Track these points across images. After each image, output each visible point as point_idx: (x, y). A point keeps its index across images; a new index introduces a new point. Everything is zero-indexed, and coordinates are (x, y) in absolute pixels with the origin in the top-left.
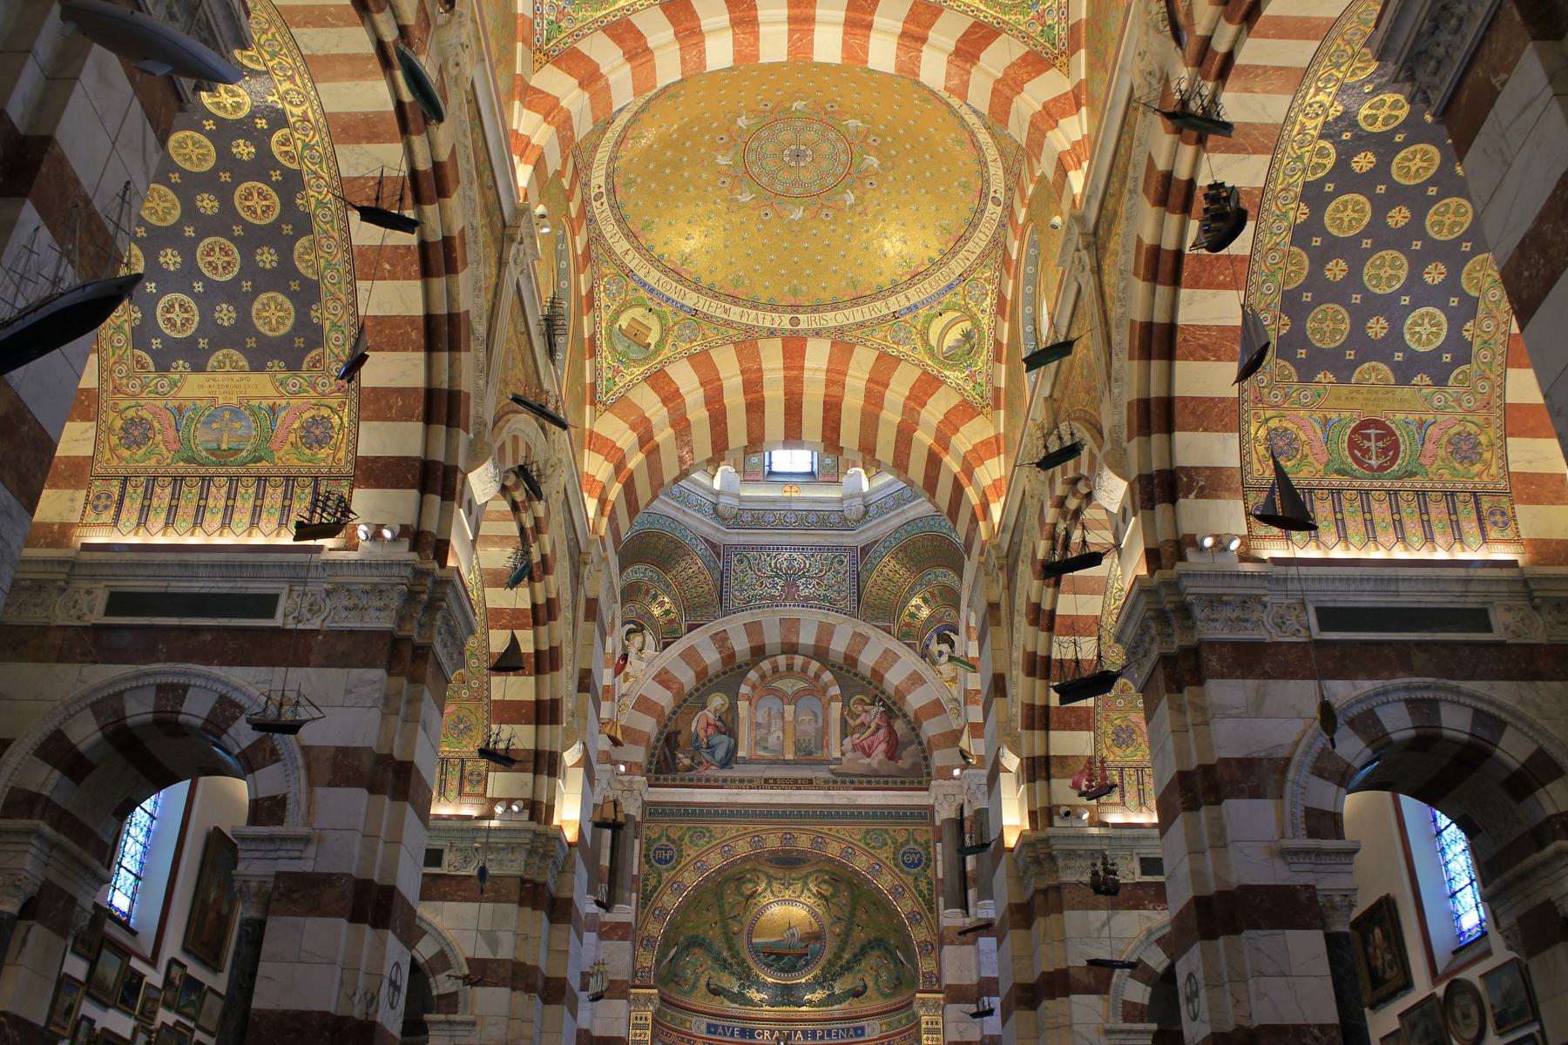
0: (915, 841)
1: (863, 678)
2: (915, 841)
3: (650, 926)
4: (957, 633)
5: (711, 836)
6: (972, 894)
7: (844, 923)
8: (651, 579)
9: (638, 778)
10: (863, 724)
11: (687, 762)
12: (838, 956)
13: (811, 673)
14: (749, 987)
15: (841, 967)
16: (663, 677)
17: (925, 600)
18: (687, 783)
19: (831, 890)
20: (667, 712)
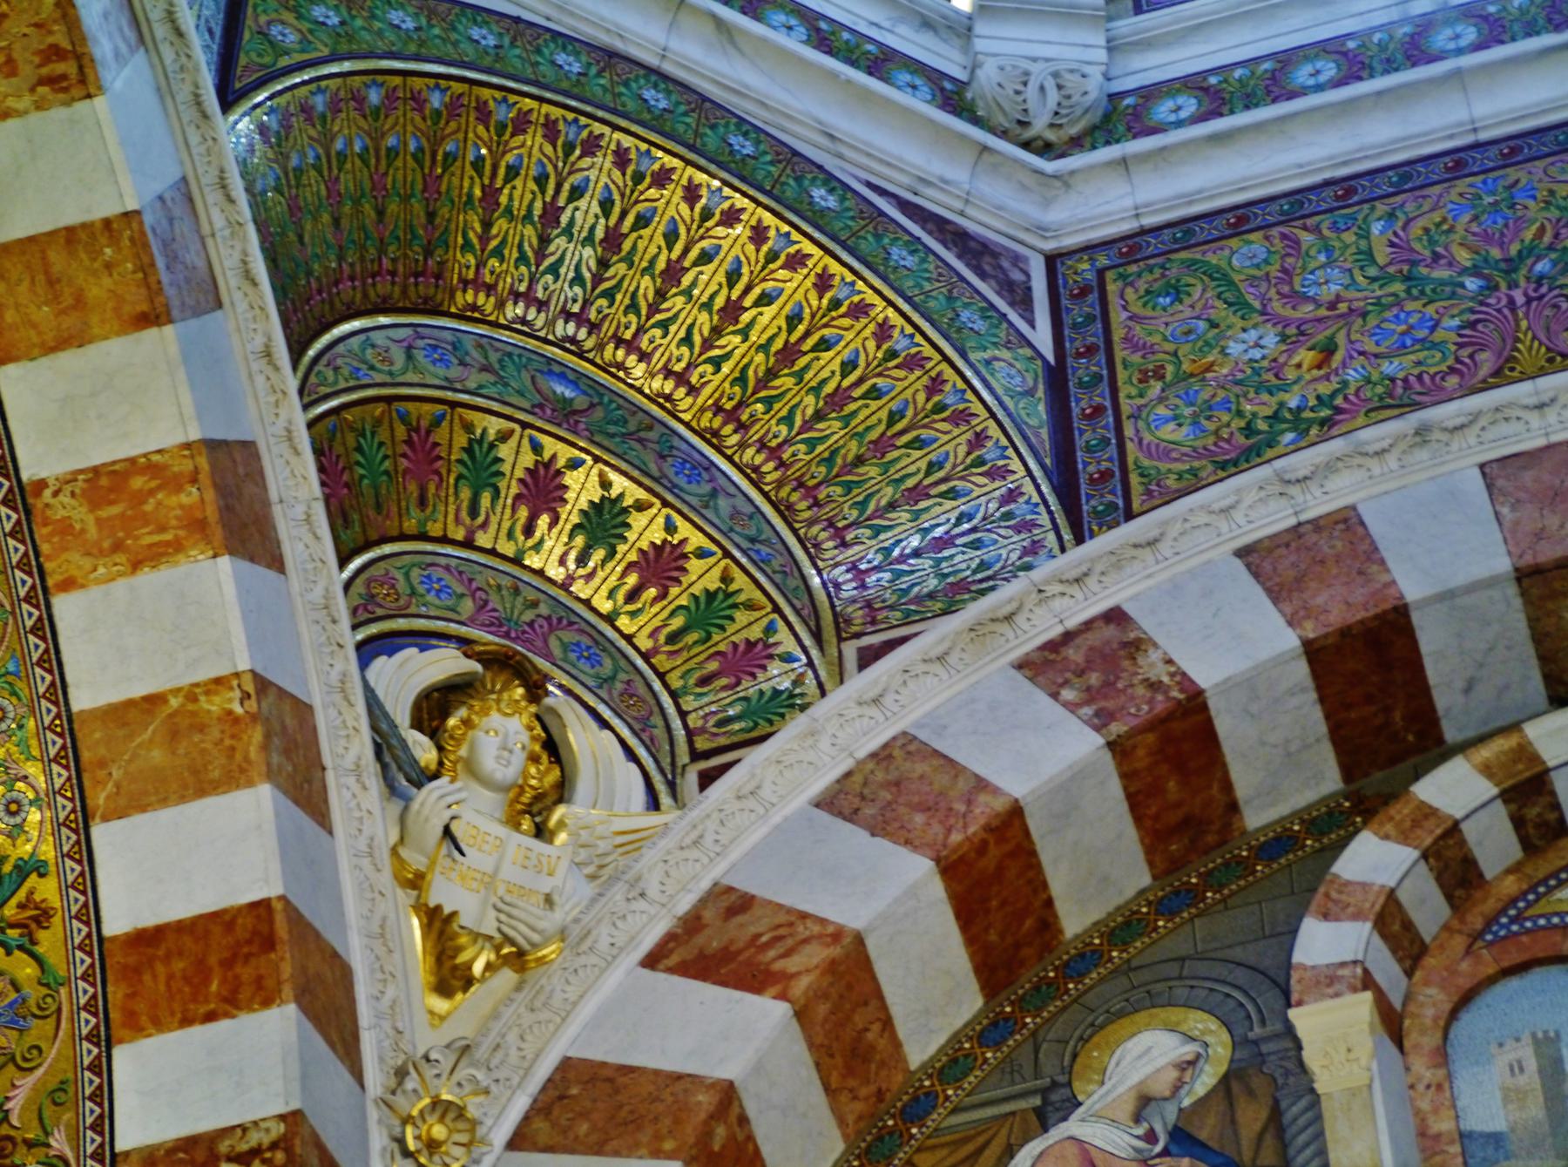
16: (711, 940)
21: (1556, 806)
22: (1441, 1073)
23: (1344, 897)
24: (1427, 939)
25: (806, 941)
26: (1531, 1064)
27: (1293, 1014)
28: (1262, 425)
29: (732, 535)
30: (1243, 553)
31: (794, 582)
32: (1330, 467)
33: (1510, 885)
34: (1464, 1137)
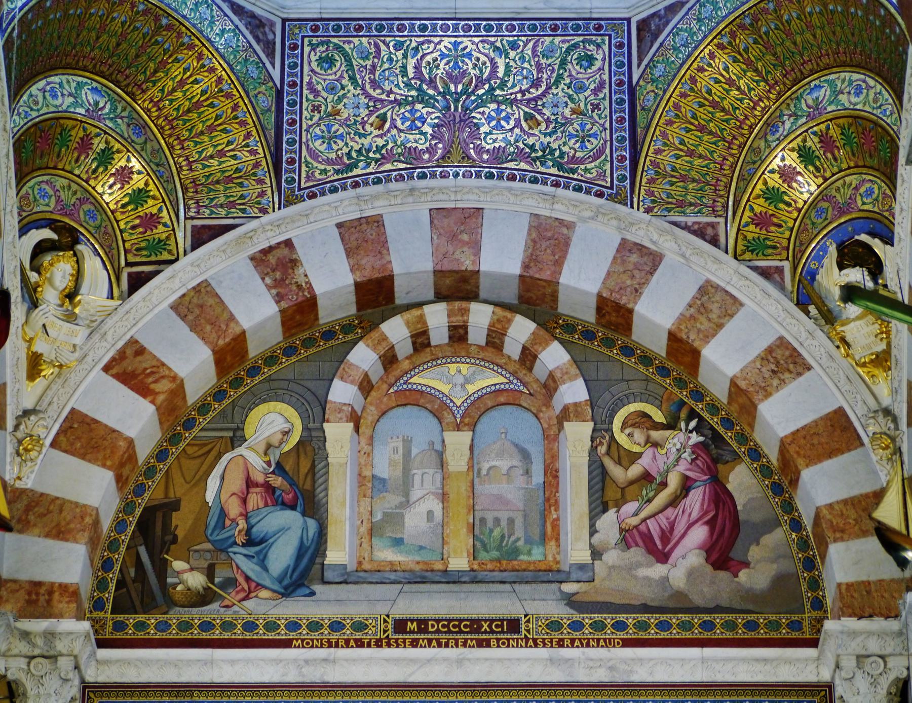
1: (646, 359)
4: (888, 240)
8: (94, 111)
9: (69, 625)
10: (647, 477)
11: (196, 580)
13: (513, 348)
16: (129, 365)
17: (806, 156)
18: (196, 633)
20: (143, 453)
21: (429, 339)
22: (370, 448)
23: (349, 371)
24: (374, 383)
25: (163, 377)
26: (401, 451)
27: (325, 425)
28: (354, 155)
29: (151, 164)
30: (339, 226)
31: (171, 186)
32: (376, 197)
33: (406, 365)
34: (373, 476)
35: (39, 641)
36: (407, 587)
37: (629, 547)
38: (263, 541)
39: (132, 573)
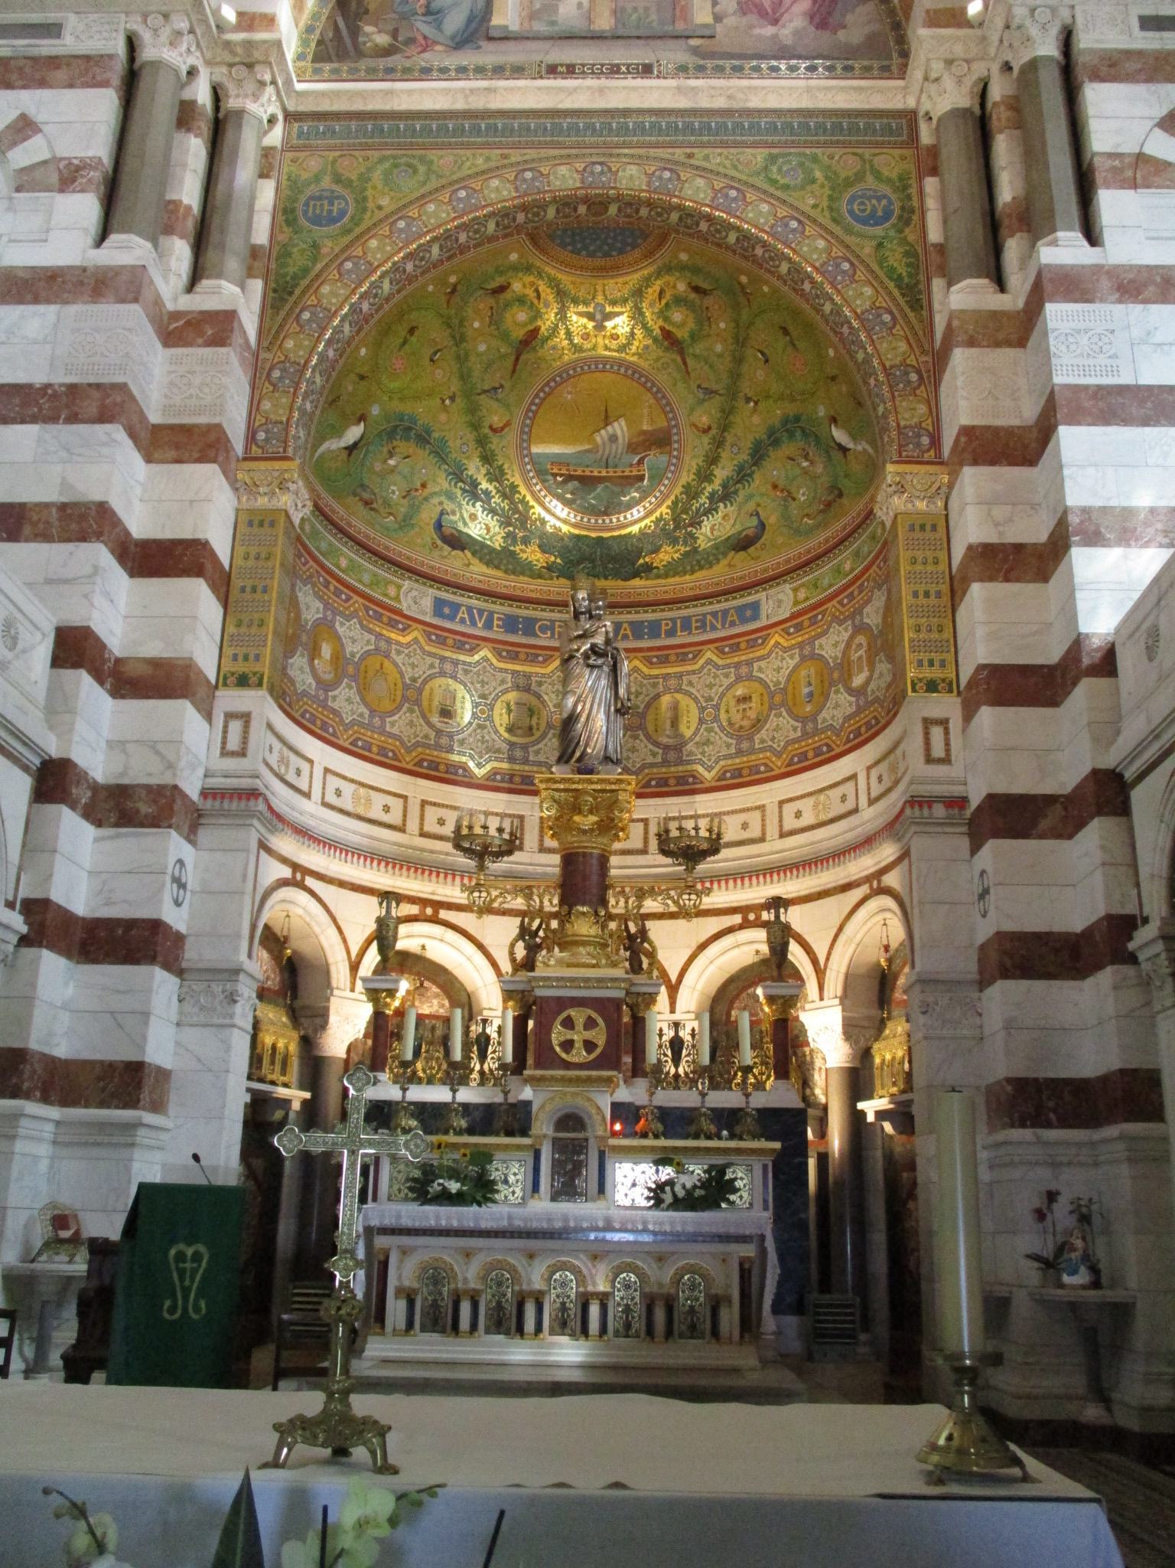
0: (877, 175)
2: (877, 175)
3: (290, 344)
5: (429, 171)
6: (1013, 248)
7: (717, 401)
11: (383, 39)
12: (705, 476)
14: (526, 541)
15: (711, 497)
19: (691, 324)
35: (239, 50)
36: (559, 42)
37: (745, 14)
38: (438, 13)
39: (331, 35)
